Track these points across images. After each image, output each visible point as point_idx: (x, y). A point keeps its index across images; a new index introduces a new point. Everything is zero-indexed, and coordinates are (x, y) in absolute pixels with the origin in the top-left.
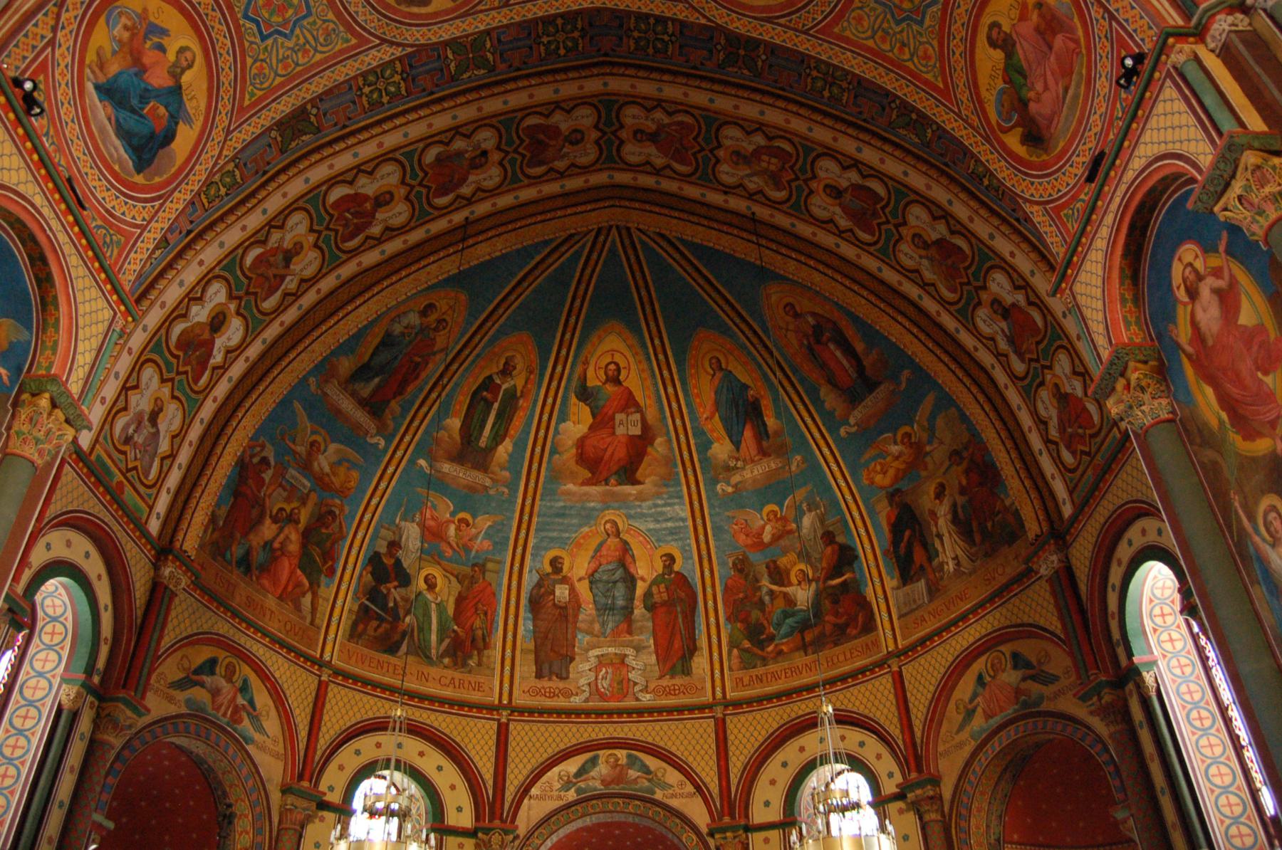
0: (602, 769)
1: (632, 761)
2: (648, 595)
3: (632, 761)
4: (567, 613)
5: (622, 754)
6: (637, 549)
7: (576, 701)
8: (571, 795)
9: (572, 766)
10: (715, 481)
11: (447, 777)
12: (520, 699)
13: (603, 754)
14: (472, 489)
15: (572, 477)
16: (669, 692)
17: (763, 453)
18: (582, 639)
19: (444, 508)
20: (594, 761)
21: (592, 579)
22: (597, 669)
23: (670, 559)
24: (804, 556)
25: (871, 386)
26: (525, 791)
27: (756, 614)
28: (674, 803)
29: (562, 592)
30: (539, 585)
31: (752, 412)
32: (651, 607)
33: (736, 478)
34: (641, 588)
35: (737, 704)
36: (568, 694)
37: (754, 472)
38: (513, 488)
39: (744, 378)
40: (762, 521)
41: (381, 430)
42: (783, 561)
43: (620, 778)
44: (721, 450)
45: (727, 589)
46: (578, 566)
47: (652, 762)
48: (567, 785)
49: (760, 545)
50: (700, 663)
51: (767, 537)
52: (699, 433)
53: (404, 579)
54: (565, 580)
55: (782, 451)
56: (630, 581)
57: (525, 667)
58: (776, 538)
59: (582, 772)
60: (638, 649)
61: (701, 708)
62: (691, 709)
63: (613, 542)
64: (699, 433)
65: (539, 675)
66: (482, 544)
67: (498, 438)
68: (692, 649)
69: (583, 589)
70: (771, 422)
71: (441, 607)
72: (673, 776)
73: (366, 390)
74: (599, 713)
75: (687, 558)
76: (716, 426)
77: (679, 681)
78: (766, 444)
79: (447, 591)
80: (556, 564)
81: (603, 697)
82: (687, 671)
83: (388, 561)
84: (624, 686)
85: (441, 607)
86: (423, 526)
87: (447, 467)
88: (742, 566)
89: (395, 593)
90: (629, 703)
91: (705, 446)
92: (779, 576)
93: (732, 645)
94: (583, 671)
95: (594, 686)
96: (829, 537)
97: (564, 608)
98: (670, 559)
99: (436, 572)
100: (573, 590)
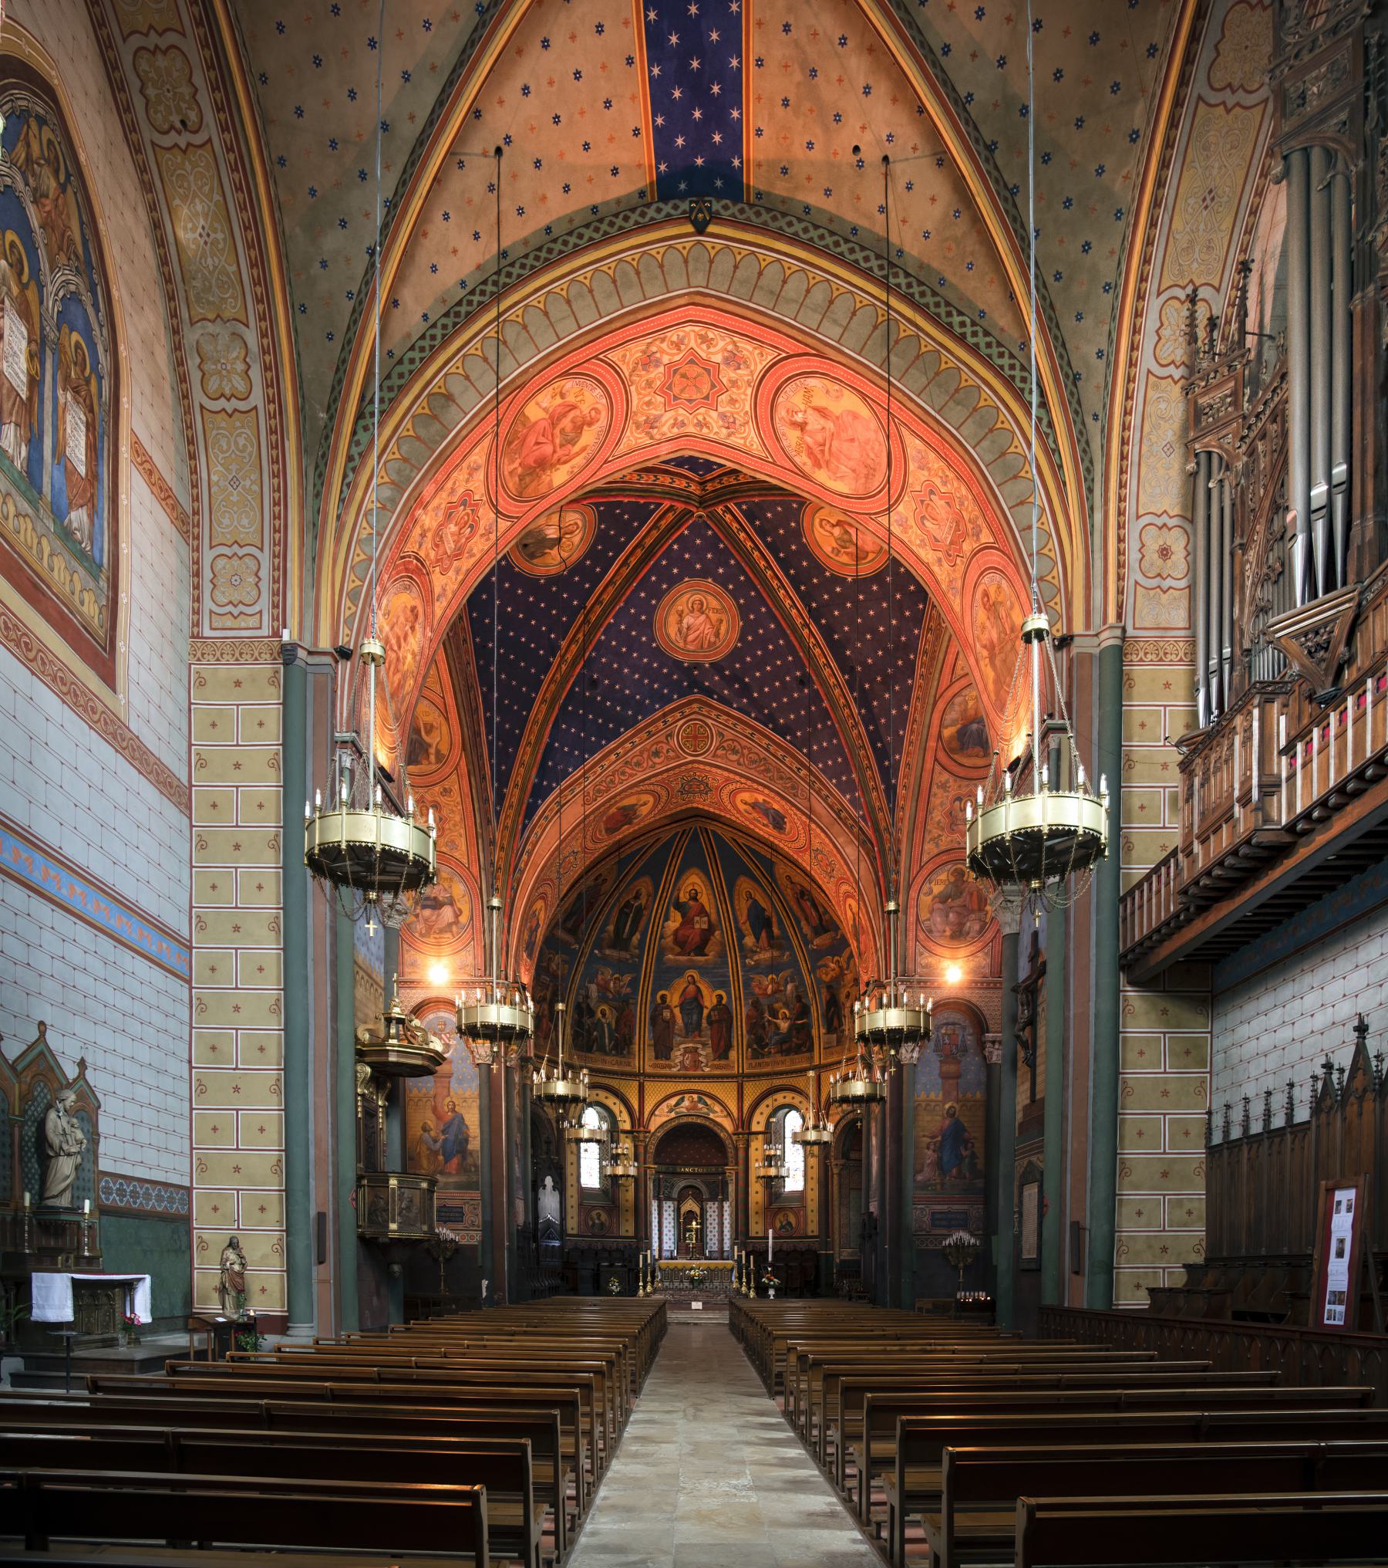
0: (686, 1103)
1: (700, 1100)
2: (709, 1016)
3: (700, 1100)
4: (670, 1024)
5: (695, 1096)
6: (705, 991)
7: (675, 1070)
8: (673, 1115)
9: (673, 1101)
10: (744, 957)
11: (617, 1107)
12: (648, 1070)
13: (687, 1096)
14: (620, 960)
15: (672, 951)
16: (718, 1067)
17: (771, 946)
18: (677, 1039)
19: (608, 973)
20: (682, 1099)
21: (682, 1006)
22: (683, 1055)
23: (720, 997)
24: (786, 1005)
25: (826, 931)
26: (652, 1113)
27: (760, 1031)
28: (718, 1120)
29: (667, 1014)
30: (655, 1010)
31: (767, 924)
32: (710, 1023)
33: (756, 958)
34: (706, 1012)
35: (750, 1076)
36: (670, 1067)
37: (765, 956)
38: (641, 957)
39: (764, 905)
40: (767, 983)
41: (579, 941)
42: (776, 1006)
43: (695, 1108)
44: (749, 941)
45: (748, 1016)
46: (674, 999)
47: (709, 1101)
48: (671, 1111)
49: (765, 994)
50: (733, 1054)
51: (769, 991)
52: (739, 930)
53: (591, 1013)
54: (668, 1007)
55: (779, 947)
56: (701, 1007)
57: (650, 1053)
58: (774, 992)
59: (677, 1104)
60: (704, 1045)
61: (732, 1077)
62: (728, 1077)
63: (692, 988)
64: (739, 930)
65: (657, 1058)
66: (627, 990)
67: (632, 933)
68: (729, 1046)
69: (677, 1011)
70: (776, 930)
71: (609, 1025)
72: (717, 1108)
73: (569, 924)
74: (685, 1077)
75: (729, 997)
76: (746, 928)
77: (723, 1062)
78: (773, 943)
79: (611, 1017)
80: (663, 997)
81: (686, 1069)
82: (727, 1058)
83: (584, 1006)
84: (696, 1064)
85: (609, 1025)
86: (598, 985)
87: (607, 952)
88: (756, 1005)
89: (587, 1021)
90: (699, 1072)
91: (741, 936)
92: (774, 1014)
93: (749, 1046)
94: (677, 1055)
95: (682, 1063)
96: (799, 998)
97: (668, 1022)
98: (720, 997)
99: (604, 1007)
100: (672, 1012)
